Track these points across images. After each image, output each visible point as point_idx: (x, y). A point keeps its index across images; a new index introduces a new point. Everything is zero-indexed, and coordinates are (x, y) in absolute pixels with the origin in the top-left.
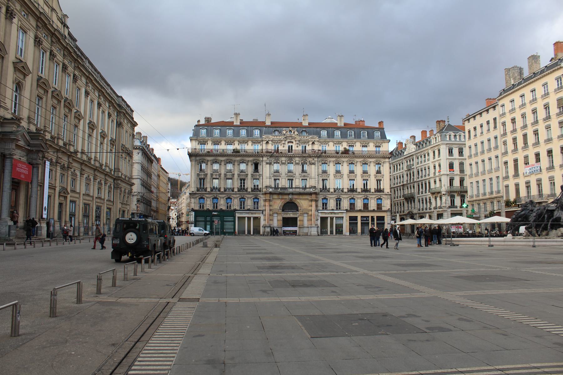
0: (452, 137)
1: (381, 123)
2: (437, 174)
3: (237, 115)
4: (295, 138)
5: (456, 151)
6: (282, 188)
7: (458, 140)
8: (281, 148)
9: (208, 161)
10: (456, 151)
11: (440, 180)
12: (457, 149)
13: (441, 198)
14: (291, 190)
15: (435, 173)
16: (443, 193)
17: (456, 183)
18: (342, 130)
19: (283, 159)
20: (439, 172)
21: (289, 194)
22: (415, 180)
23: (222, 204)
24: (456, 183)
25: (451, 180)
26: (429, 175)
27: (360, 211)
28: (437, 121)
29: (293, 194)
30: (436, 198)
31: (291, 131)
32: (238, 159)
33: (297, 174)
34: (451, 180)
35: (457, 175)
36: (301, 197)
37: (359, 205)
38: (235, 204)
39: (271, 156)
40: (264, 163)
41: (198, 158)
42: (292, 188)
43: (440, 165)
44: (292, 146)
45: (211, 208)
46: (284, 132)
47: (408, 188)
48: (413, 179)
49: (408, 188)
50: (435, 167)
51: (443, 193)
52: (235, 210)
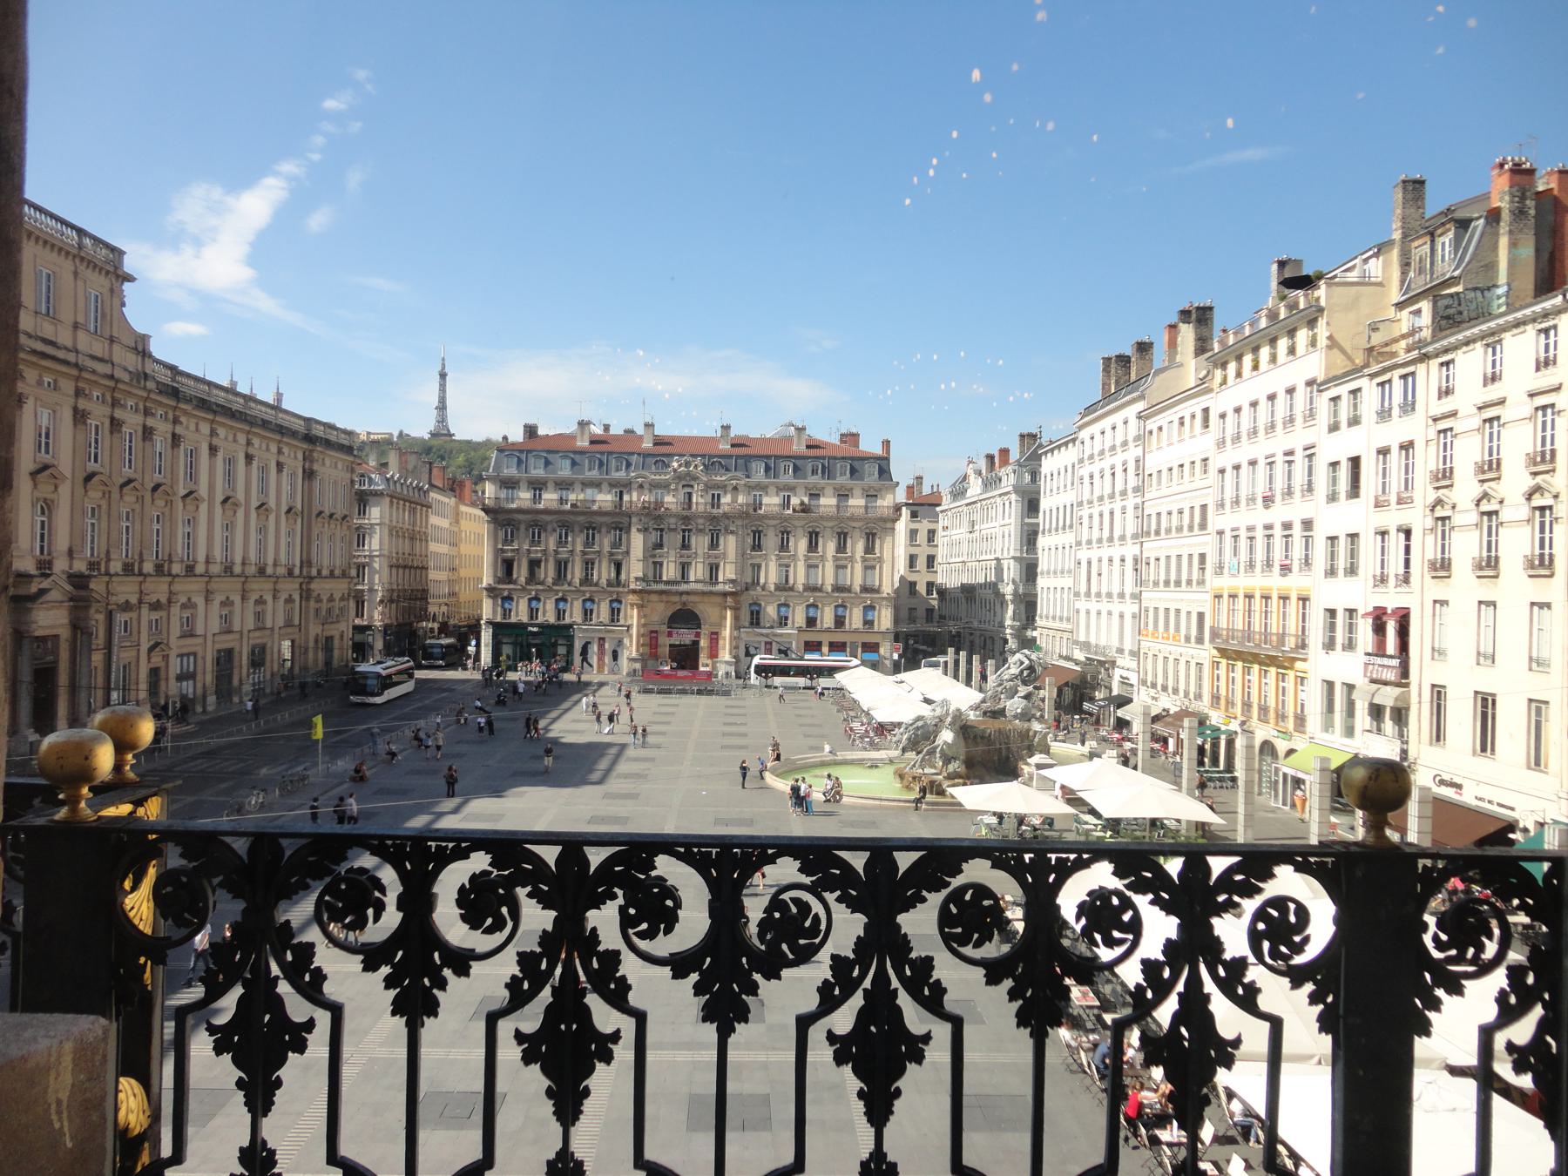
1: (886, 444)
3: (583, 424)
4: (695, 478)
6: (667, 583)
8: (669, 499)
9: (520, 522)
14: (684, 587)
18: (799, 462)
19: (672, 520)
21: (681, 594)
23: (548, 615)
27: (828, 630)
28: (1022, 436)
29: (688, 593)
31: (687, 464)
32: (581, 519)
33: (700, 552)
36: (706, 599)
37: (827, 618)
38: (574, 615)
39: (647, 515)
40: (634, 530)
41: (501, 517)
42: (661, 581)
44: (690, 494)
45: (525, 619)
46: (675, 465)
52: (575, 623)
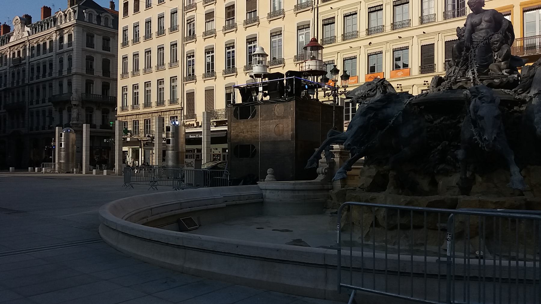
0: (94, 18)
2: (65, 73)
5: (98, 41)
7: (102, 23)
10: (98, 41)
11: (70, 84)
12: (102, 37)
13: (69, 111)
15: (61, 72)
16: (73, 103)
17: (97, 89)
20: (69, 69)
22: (26, 82)
24: (97, 89)
25: (89, 84)
26: (50, 74)
30: (61, 112)
34: (89, 84)
35: (98, 77)
43: (70, 59)
47: (13, 95)
48: (23, 80)
49: (13, 95)
50: (61, 61)
51: (73, 103)
